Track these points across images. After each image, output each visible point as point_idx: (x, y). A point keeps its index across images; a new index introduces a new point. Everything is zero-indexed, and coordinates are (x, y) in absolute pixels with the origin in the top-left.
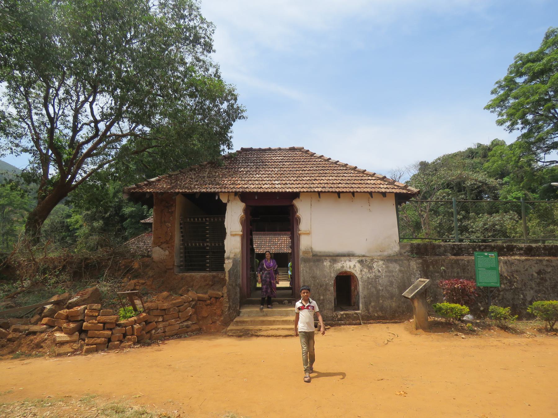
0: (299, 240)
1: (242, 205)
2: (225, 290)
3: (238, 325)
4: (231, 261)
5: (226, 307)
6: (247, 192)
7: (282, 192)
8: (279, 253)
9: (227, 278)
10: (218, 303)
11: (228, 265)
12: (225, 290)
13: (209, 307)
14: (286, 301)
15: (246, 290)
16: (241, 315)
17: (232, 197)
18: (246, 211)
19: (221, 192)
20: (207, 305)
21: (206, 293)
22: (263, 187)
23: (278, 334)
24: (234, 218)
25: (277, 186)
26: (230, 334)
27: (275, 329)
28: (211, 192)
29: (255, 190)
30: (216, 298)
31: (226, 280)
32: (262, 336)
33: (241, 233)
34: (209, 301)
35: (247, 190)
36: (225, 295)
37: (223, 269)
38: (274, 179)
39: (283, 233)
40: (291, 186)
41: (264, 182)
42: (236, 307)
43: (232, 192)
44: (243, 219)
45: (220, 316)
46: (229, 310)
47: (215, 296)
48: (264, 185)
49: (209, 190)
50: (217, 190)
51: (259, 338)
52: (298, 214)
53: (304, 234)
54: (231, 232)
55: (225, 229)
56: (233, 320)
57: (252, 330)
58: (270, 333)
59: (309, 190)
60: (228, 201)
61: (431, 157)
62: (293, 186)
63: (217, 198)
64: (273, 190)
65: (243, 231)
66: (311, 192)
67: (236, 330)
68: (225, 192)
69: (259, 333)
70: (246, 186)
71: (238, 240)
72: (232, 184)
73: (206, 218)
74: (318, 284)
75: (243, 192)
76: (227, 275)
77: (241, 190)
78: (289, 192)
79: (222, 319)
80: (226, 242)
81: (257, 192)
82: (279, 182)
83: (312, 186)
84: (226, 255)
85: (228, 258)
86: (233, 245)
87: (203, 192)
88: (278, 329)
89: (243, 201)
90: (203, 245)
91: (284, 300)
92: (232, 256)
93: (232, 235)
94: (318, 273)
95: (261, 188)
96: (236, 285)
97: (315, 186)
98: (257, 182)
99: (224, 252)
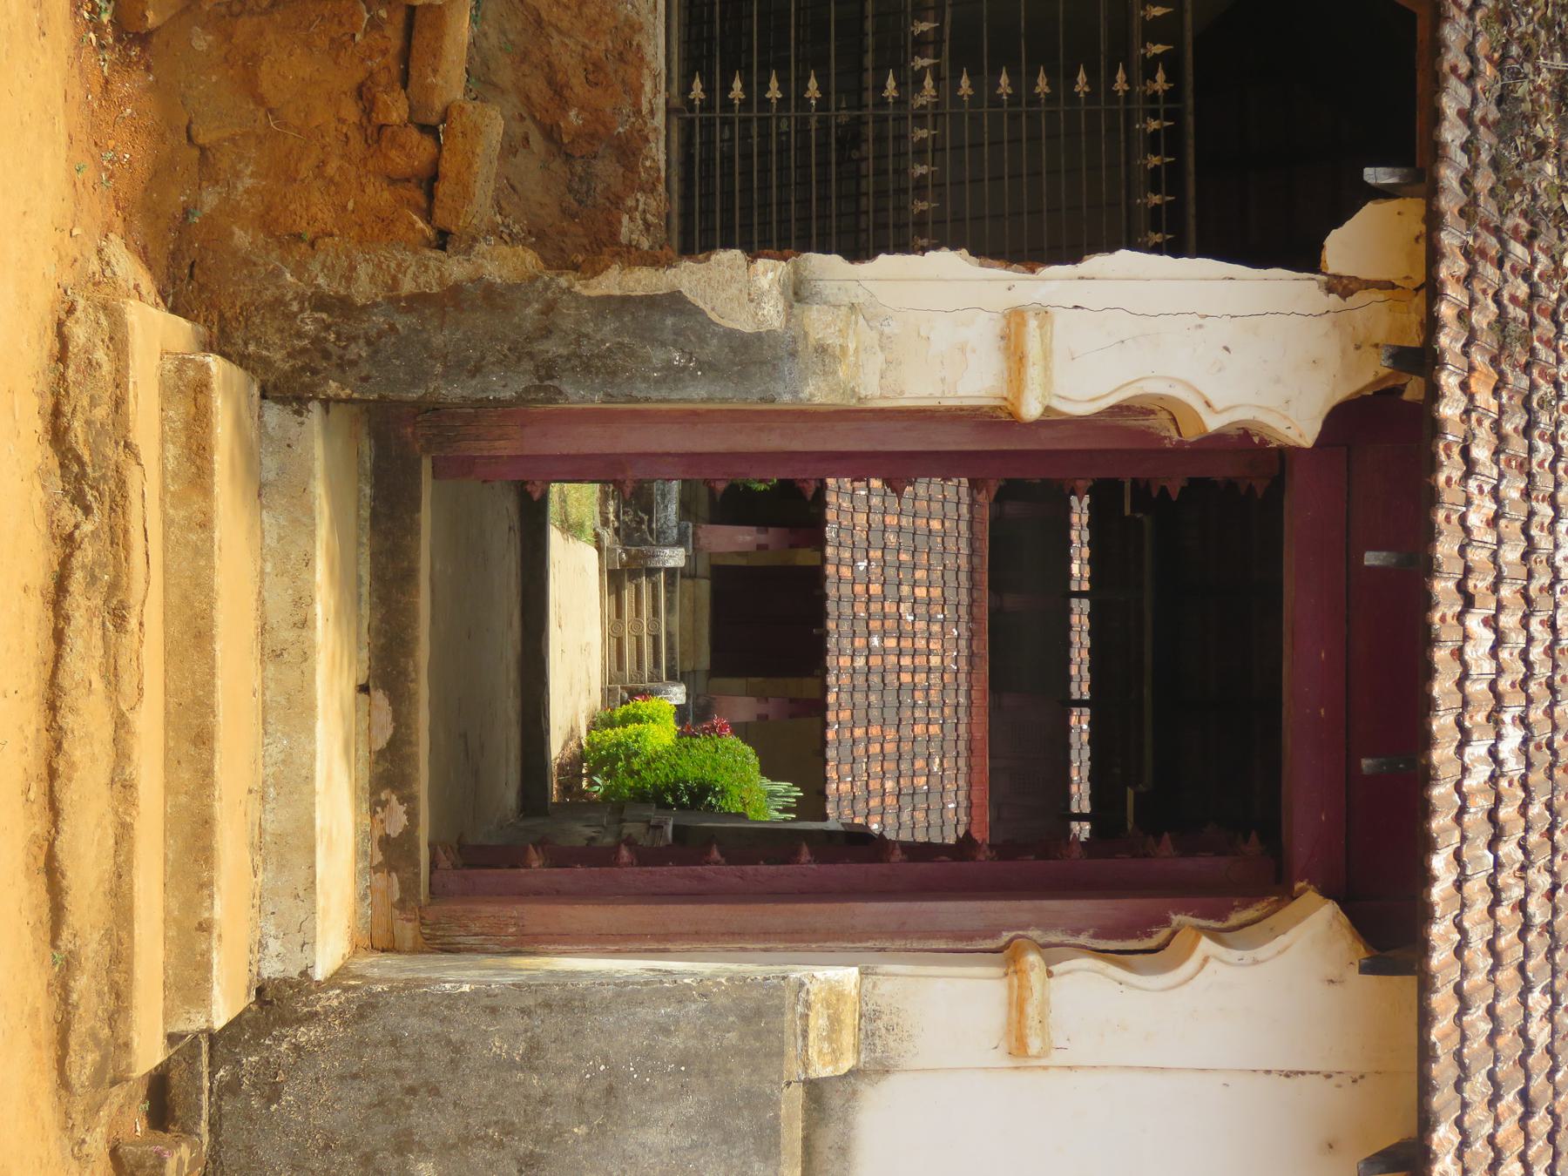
0: (963, 944)
1: (1297, 420)
2: (502, 263)
3: (168, 393)
4: (771, 314)
5: (349, 277)
6: (1434, 465)
7: (1425, 810)
8: (822, 615)
9: (613, 282)
10: (381, 196)
11: (740, 290)
12: (502, 263)
13: (351, 112)
14: (397, 821)
15: (504, 448)
16: (275, 415)
17: (1382, 320)
18: (1245, 448)
19: (1434, 221)
20: (364, 94)
21: (481, 81)
22: (1474, 621)
23: (69, 796)
24: (1181, 340)
25: (1477, 750)
26: (79, 333)
27: (121, 755)
28: (1437, 117)
29: (1445, 548)
30: (430, 180)
31: (593, 269)
32: (58, 637)
33: (1031, 410)
34: (395, 109)
35: (1451, 469)
36: (456, 269)
37: (696, 236)
38: (1536, 714)
39: (983, 646)
40: (1477, 887)
41: (1509, 621)
42: (344, 365)
43: (1432, 325)
44: (1160, 423)
45: (267, 223)
46: (321, 302)
47: (448, 167)
48: (1492, 622)
49: (1453, 100)
50: (1449, 176)
51: (35, 610)
52: (1206, 945)
53: (1018, 1005)
54: (1044, 313)
55: (1075, 258)
56: (219, 342)
57: (117, 538)
58: (88, 718)
59: (1443, 1070)
60: (1341, 287)
62: (1481, 903)
63: (1375, 175)
64: (1442, 723)
65: (1052, 422)
66: (1425, 1087)
67: (120, 383)
68: (1434, 255)
69: (81, 603)
70: (1481, 453)
71: (973, 382)
72: (1502, 319)
73: (1172, 64)
74: (554, 1136)
75: (1436, 428)
76: (643, 281)
77: (1450, 410)
78: (1428, 879)
79: (242, 238)
80: (948, 266)
81: (1429, 568)
82: (1514, 766)
83: (1478, 1087)
84: (827, 267)
85: (798, 293)
86: (924, 329)
87: (1438, 47)
88: (123, 787)
89: (1346, 420)
90: (920, 44)
91: (409, 800)
92: (819, 323)
93: (1015, 319)
94: (654, 1136)
95: (1469, 601)
96: (547, 370)
97: (1478, 1116)
98: (1511, 554)
99: (857, 252)
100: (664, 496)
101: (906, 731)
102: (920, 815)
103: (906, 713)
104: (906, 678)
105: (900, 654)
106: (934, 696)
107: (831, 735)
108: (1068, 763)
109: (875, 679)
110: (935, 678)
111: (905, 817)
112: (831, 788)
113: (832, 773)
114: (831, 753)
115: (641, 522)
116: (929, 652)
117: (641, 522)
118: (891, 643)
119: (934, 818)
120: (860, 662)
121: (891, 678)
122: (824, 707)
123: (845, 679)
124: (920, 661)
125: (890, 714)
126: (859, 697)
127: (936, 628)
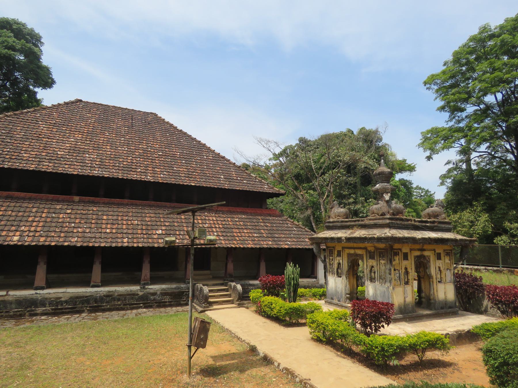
61: (313, 134)
100: (179, 288)
101: (232, 226)
102: (248, 224)
103: (228, 226)
104: (221, 226)
105: (216, 227)
106: (222, 219)
107: (242, 246)
108: (236, 190)
109: (224, 234)
110: (218, 219)
111: (250, 227)
112: (253, 246)
113: (249, 246)
114: (245, 246)
115: (186, 294)
116: (213, 220)
117: (186, 294)
118: (214, 229)
119: (247, 220)
120: (221, 238)
121: (222, 230)
122: (236, 248)
123: (227, 242)
124: (215, 222)
125: (230, 230)
126: (230, 238)
127: (207, 218)
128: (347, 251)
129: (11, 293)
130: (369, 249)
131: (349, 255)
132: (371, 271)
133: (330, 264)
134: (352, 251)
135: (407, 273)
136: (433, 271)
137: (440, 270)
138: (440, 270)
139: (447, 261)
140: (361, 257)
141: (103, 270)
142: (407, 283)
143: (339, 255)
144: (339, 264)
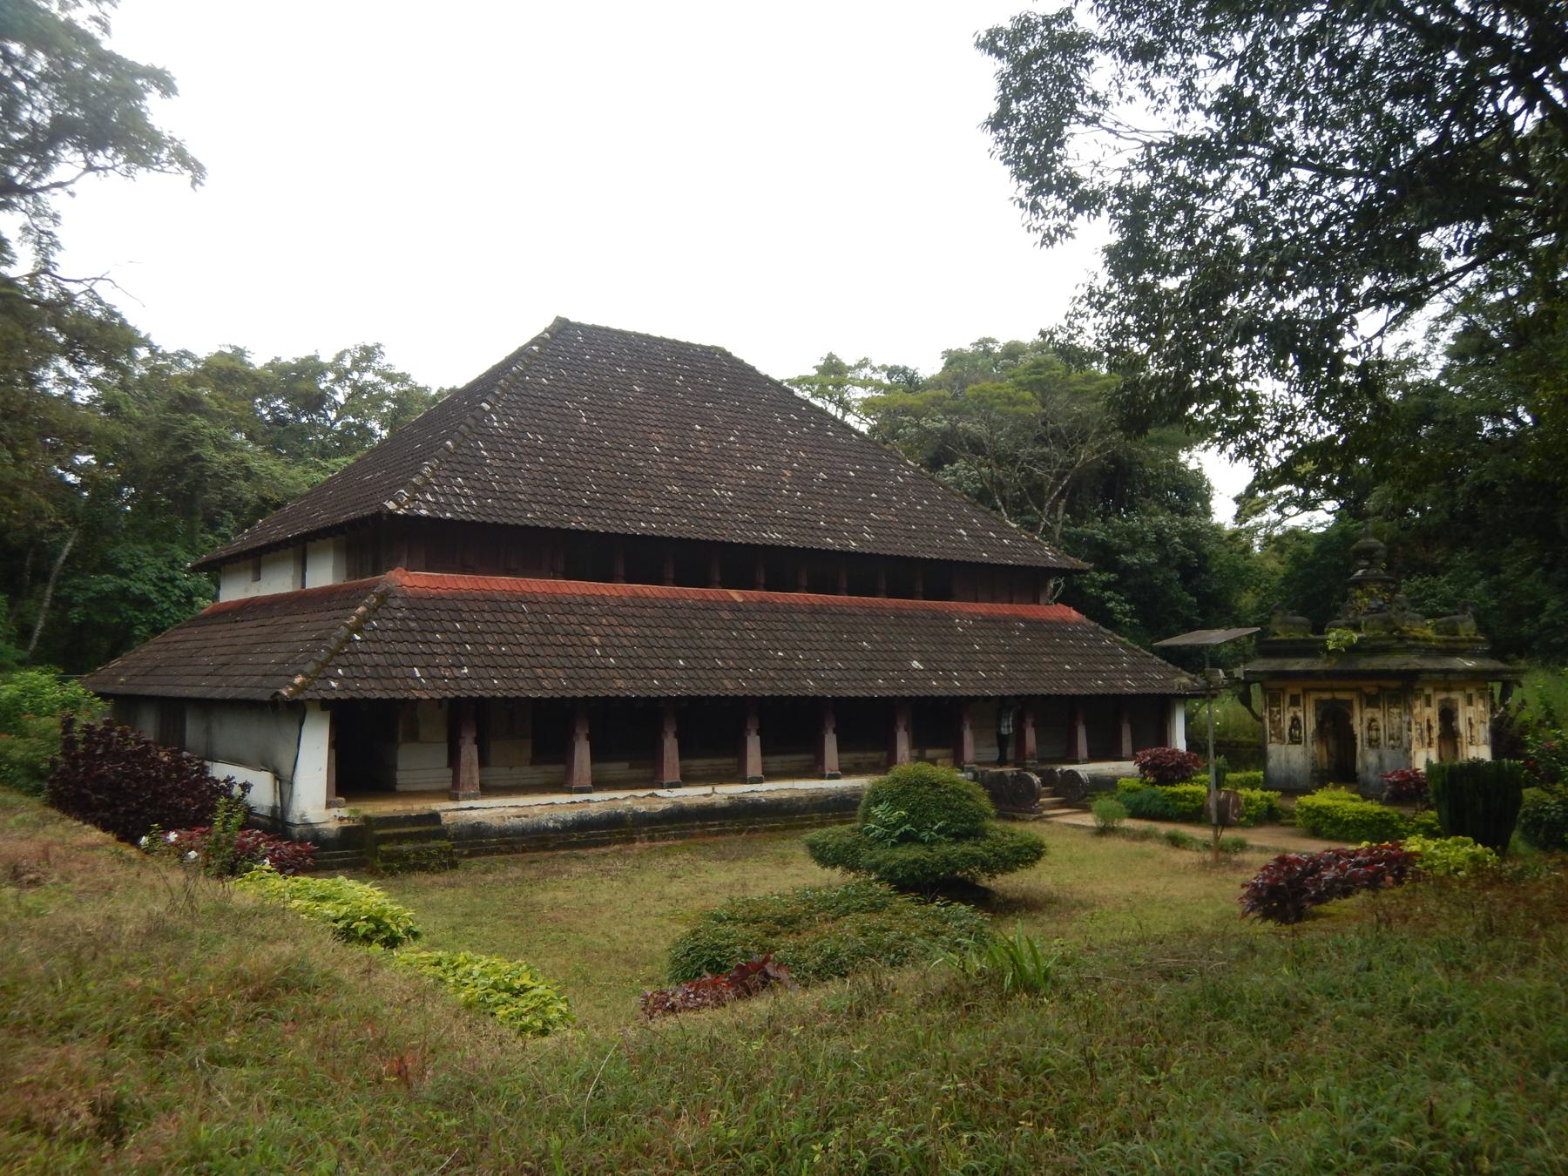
128: (1314, 696)
129: (721, 789)
130: (1366, 690)
131: (1319, 704)
132: (1369, 728)
133: (1272, 721)
134: (1326, 696)
135: (1430, 728)
136: (1462, 725)
137: (1471, 724)
138: (1471, 724)
139: (1481, 708)
140: (1350, 703)
141: (840, 750)
142: (1430, 745)
143: (1295, 702)
144: (1295, 719)
